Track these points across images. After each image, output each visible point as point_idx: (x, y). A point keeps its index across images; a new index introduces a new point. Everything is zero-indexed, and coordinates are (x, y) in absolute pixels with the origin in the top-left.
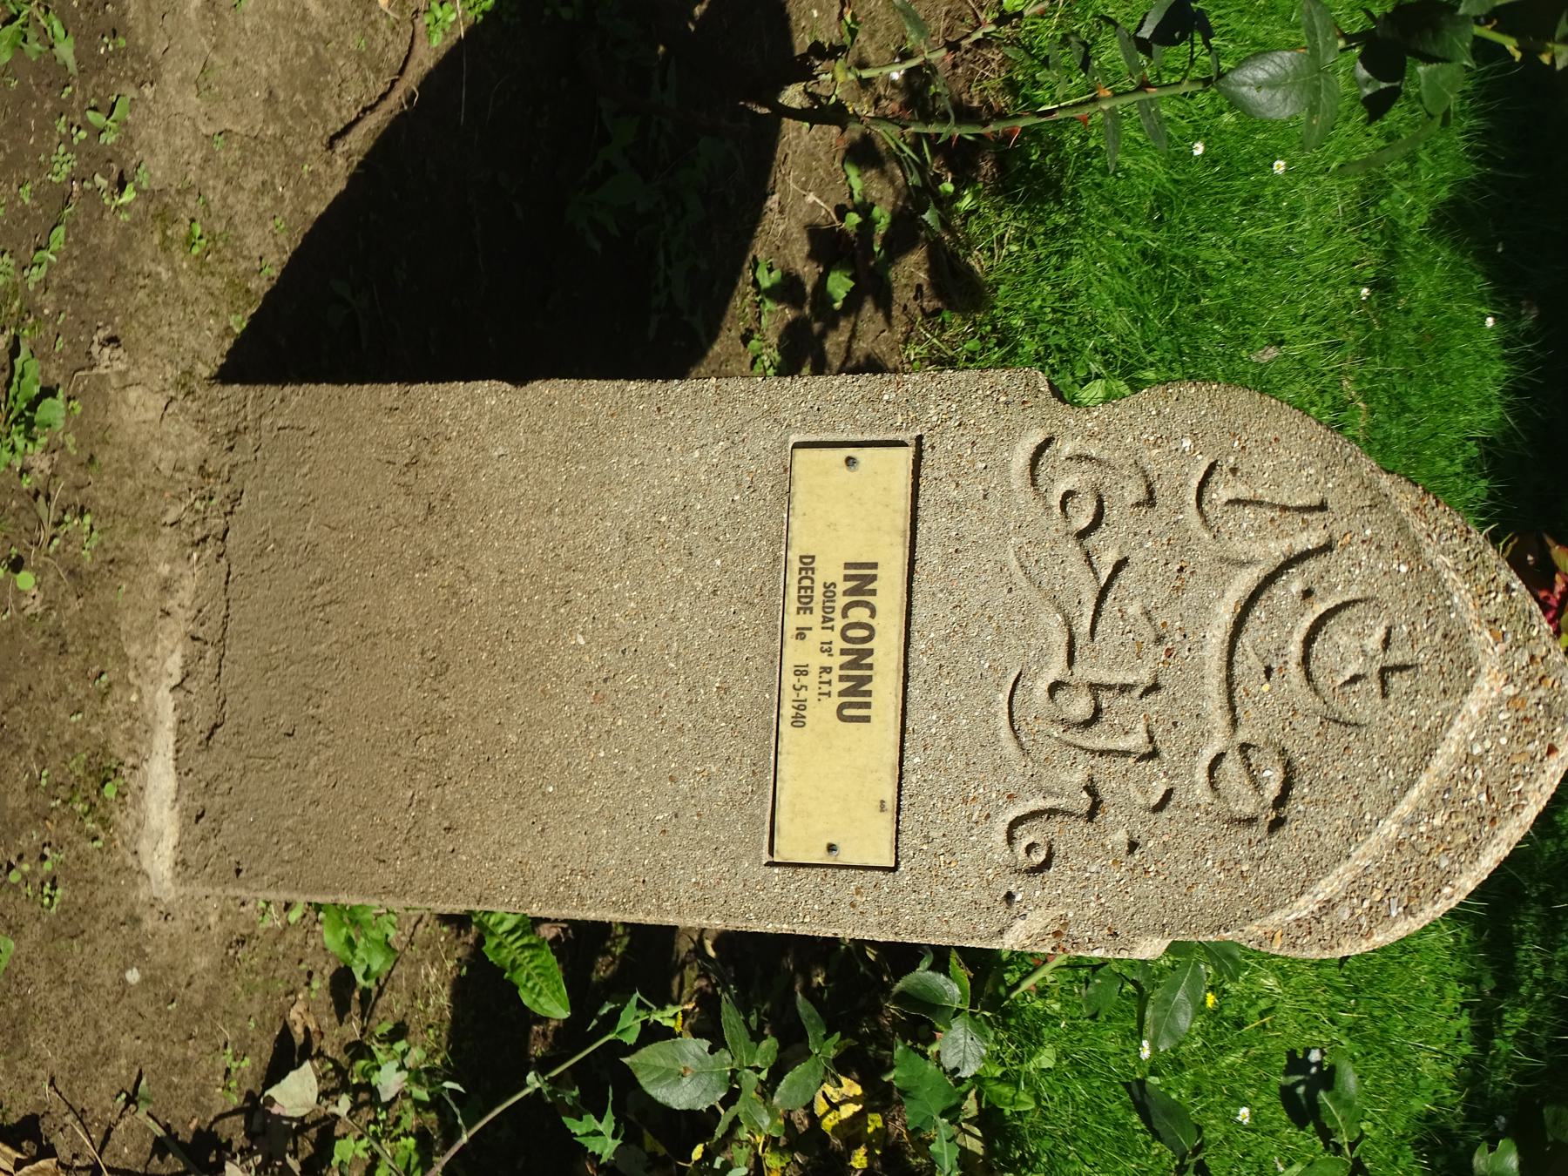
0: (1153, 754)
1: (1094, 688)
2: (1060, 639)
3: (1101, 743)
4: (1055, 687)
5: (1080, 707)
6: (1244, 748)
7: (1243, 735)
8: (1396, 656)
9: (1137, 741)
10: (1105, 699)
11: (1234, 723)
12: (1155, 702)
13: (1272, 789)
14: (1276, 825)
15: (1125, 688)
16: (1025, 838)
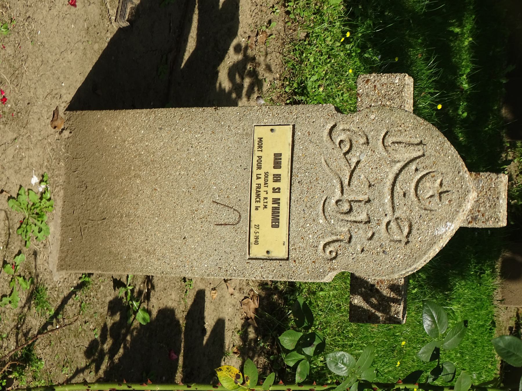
0: (369, 222)
1: (350, 202)
2: (339, 186)
3: (352, 218)
4: (337, 202)
5: (346, 207)
6: (397, 219)
7: (397, 214)
8: (444, 189)
9: (363, 217)
10: (352, 204)
11: (394, 211)
12: (368, 206)
13: (406, 231)
14: (407, 242)
15: (360, 201)
16: (329, 249)
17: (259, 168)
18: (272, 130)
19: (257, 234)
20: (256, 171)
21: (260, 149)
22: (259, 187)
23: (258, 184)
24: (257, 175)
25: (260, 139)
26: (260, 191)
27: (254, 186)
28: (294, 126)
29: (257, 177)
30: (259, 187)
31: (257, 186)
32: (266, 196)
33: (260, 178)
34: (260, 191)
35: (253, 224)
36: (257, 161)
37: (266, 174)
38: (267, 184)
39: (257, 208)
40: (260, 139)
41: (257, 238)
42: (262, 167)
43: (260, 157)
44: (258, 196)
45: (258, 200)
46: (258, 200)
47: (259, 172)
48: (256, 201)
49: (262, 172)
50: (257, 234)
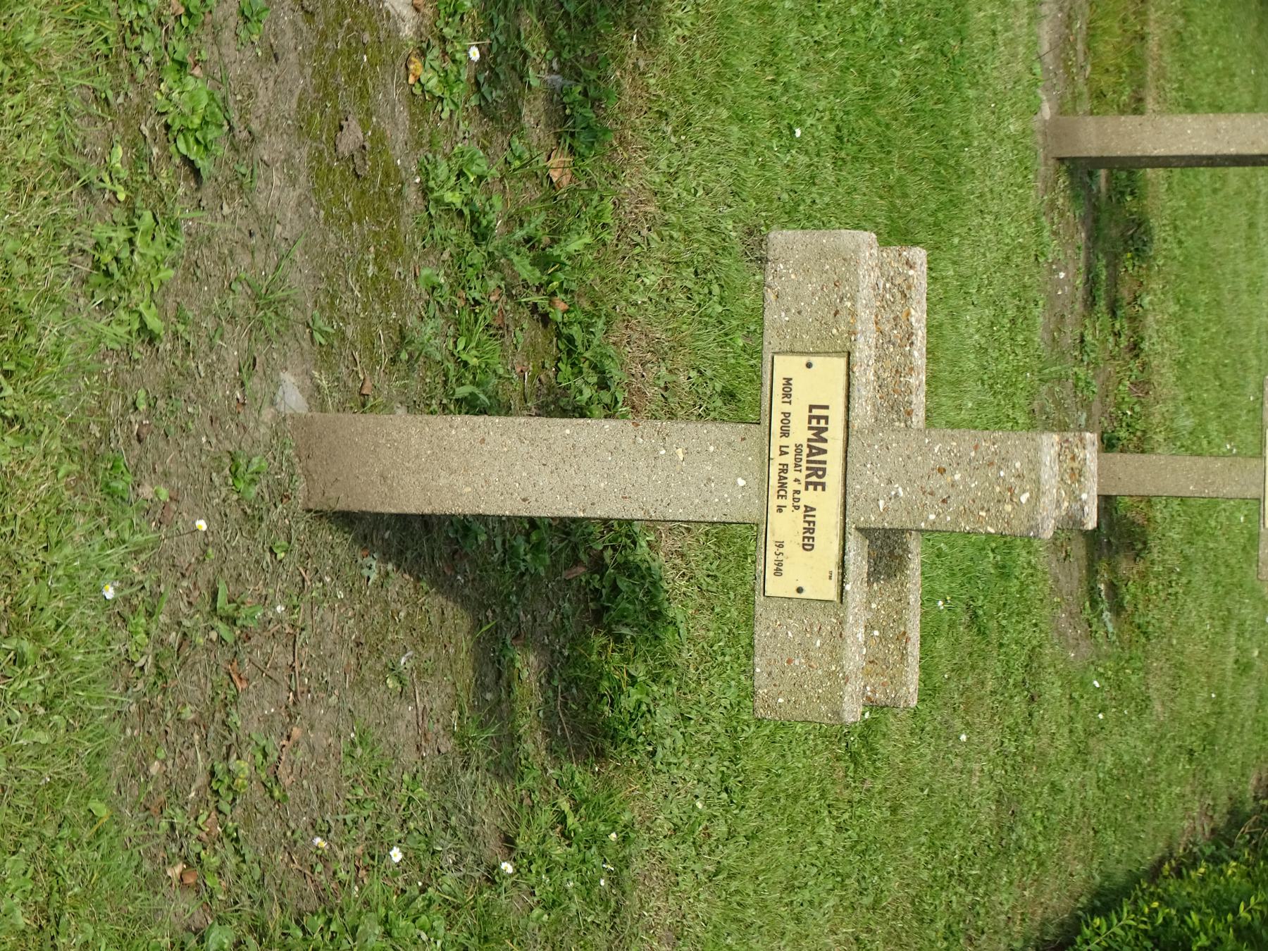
17: (785, 433)
18: (809, 365)
20: (777, 441)
22: (784, 469)
25: (788, 381)
28: (849, 354)
30: (784, 469)
32: (798, 487)
37: (798, 448)
39: (780, 509)
40: (788, 381)
41: (779, 564)
43: (787, 415)
44: (783, 486)
45: (782, 493)
46: (782, 493)
47: (784, 441)
49: (790, 442)
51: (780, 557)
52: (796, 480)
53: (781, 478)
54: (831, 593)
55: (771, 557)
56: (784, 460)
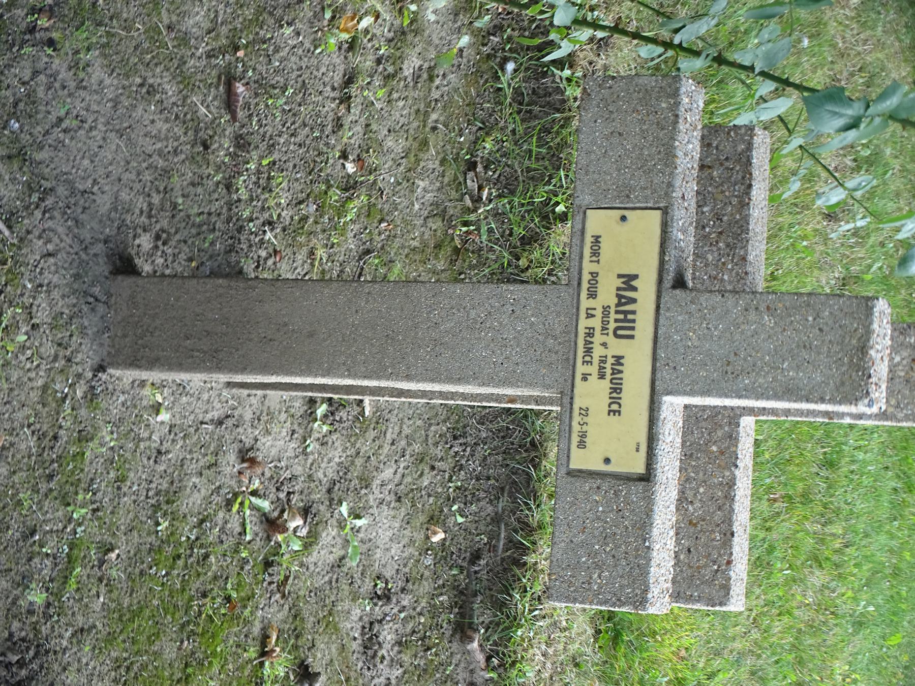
17: (592, 295)
19: (584, 430)
20: (585, 303)
21: (594, 258)
22: (590, 333)
23: (590, 329)
24: (587, 309)
26: (592, 343)
27: (582, 331)
29: (587, 314)
30: (590, 333)
31: (587, 331)
33: (593, 316)
34: (592, 343)
35: (576, 407)
36: (589, 283)
37: (606, 309)
38: (607, 329)
39: (585, 378)
40: (597, 239)
42: (598, 293)
44: (588, 351)
47: (591, 303)
48: (583, 362)
49: (597, 304)
50: (585, 428)
51: (585, 428)
52: (604, 345)
53: (587, 343)
54: (640, 469)
55: (576, 427)
56: (591, 323)
